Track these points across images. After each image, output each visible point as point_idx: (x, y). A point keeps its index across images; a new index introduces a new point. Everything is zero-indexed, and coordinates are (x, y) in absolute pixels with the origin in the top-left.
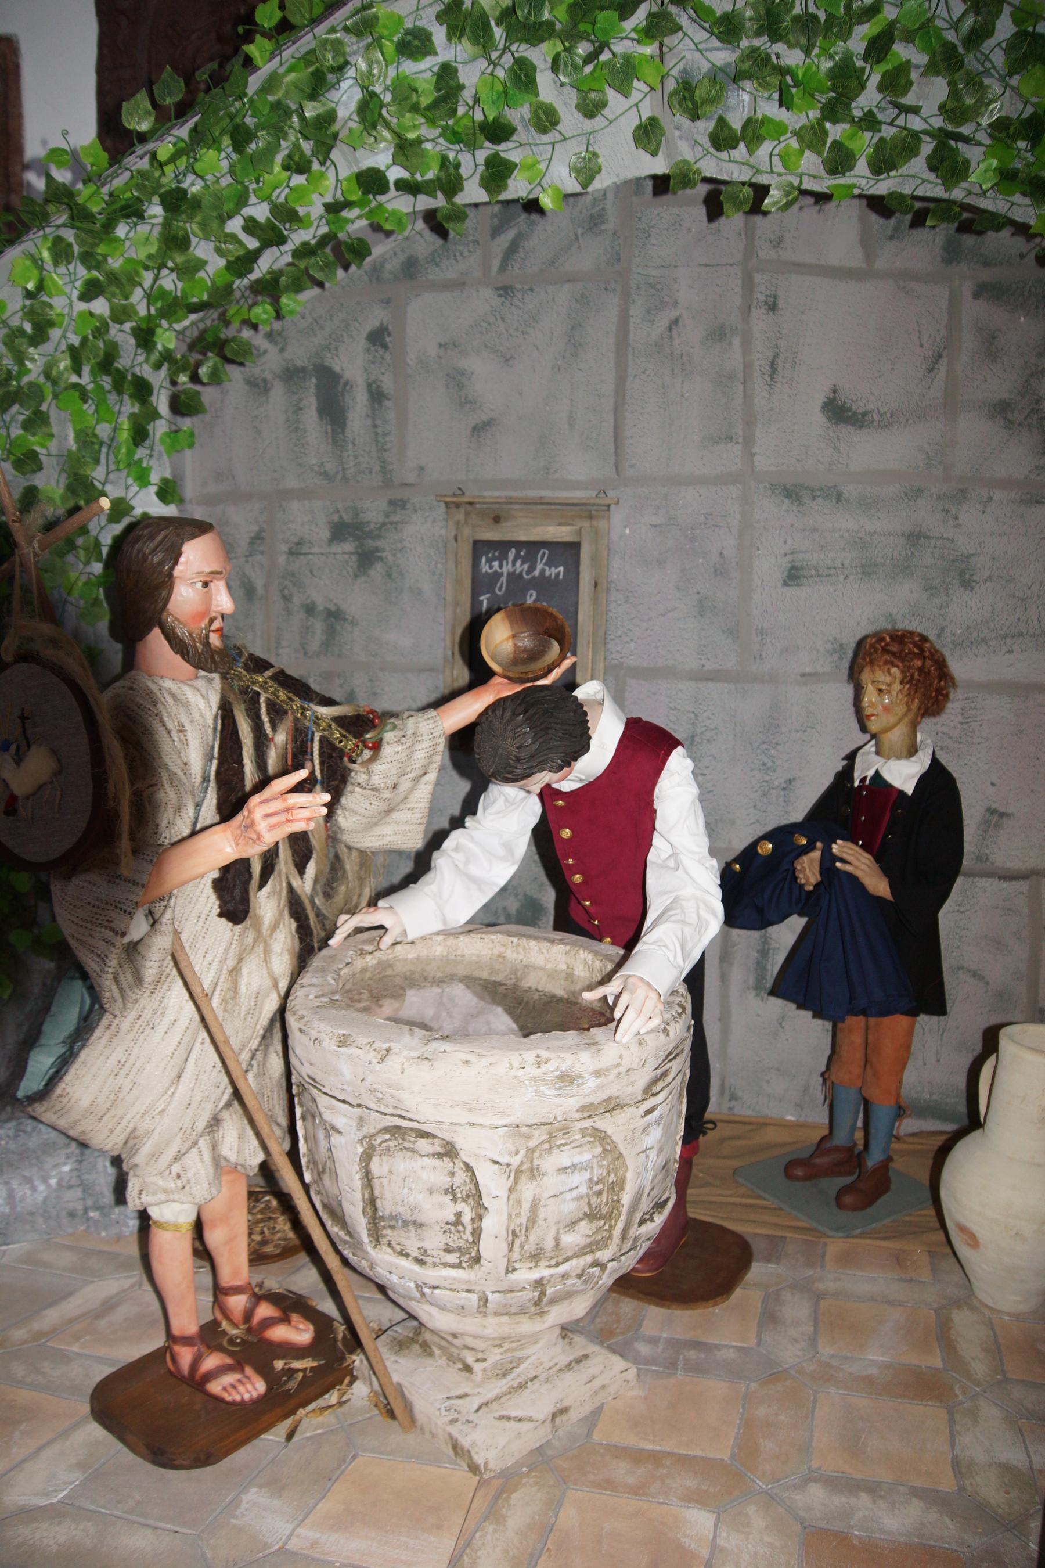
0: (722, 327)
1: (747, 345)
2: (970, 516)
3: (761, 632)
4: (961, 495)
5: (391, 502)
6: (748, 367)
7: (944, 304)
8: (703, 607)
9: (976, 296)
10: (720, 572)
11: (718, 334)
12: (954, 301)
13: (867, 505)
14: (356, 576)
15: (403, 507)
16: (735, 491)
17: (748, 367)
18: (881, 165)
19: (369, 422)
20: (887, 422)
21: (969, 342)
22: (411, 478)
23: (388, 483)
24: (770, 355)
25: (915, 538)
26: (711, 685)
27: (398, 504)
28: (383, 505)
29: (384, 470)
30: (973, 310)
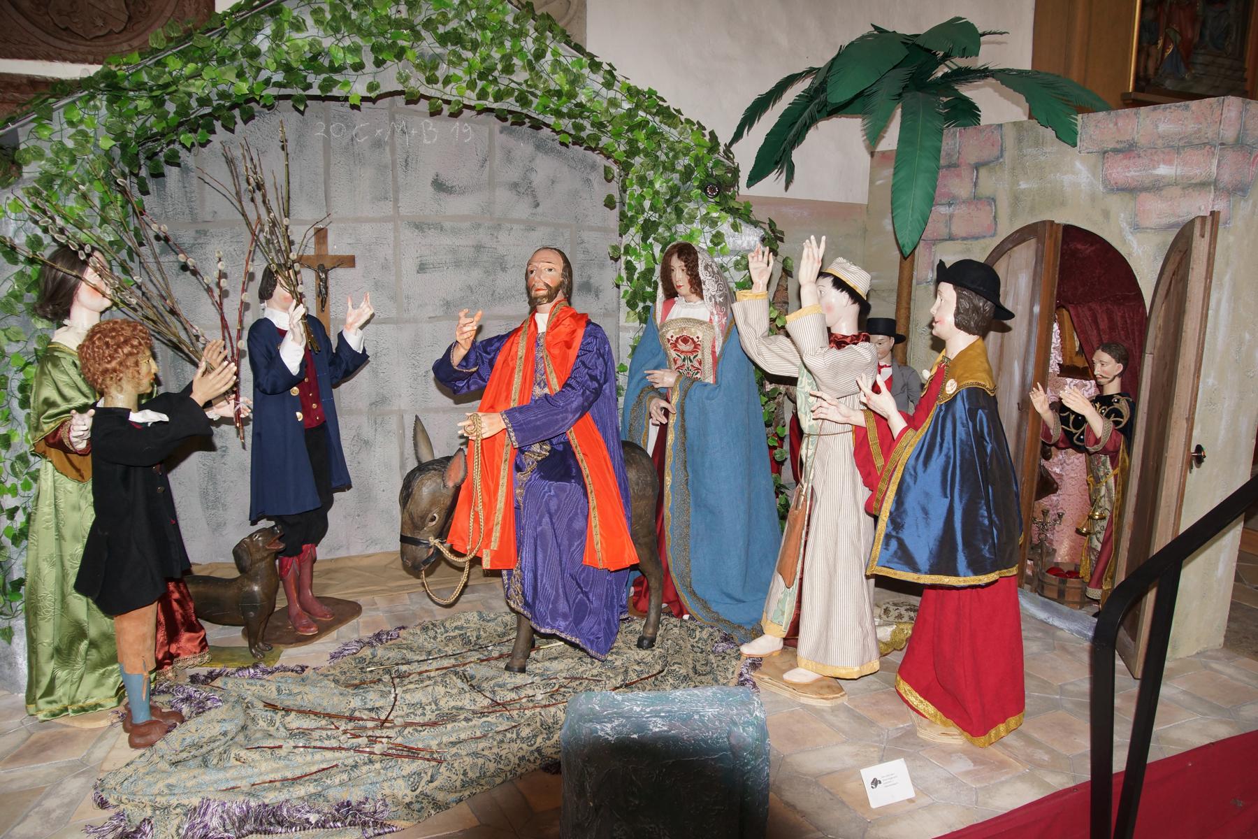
0: (380, 140)
1: (393, 151)
2: (503, 237)
3: (408, 297)
4: (498, 227)
5: (197, 232)
6: (394, 163)
7: (487, 135)
8: (377, 286)
9: (501, 132)
10: (385, 267)
11: (378, 144)
12: (491, 134)
13: (455, 232)
14: (178, 275)
15: (205, 235)
16: (390, 226)
17: (394, 163)
18: (499, 97)
19: (181, 184)
20: (463, 191)
21: (498, 155)
22: (209, 218)
23: (194, 221)
24: (405, 156)
25: (479, 248)
26: (383, 326)
27: (202, 233)
28: (193, 234)
29: (191, 213)
30: (501, 139)
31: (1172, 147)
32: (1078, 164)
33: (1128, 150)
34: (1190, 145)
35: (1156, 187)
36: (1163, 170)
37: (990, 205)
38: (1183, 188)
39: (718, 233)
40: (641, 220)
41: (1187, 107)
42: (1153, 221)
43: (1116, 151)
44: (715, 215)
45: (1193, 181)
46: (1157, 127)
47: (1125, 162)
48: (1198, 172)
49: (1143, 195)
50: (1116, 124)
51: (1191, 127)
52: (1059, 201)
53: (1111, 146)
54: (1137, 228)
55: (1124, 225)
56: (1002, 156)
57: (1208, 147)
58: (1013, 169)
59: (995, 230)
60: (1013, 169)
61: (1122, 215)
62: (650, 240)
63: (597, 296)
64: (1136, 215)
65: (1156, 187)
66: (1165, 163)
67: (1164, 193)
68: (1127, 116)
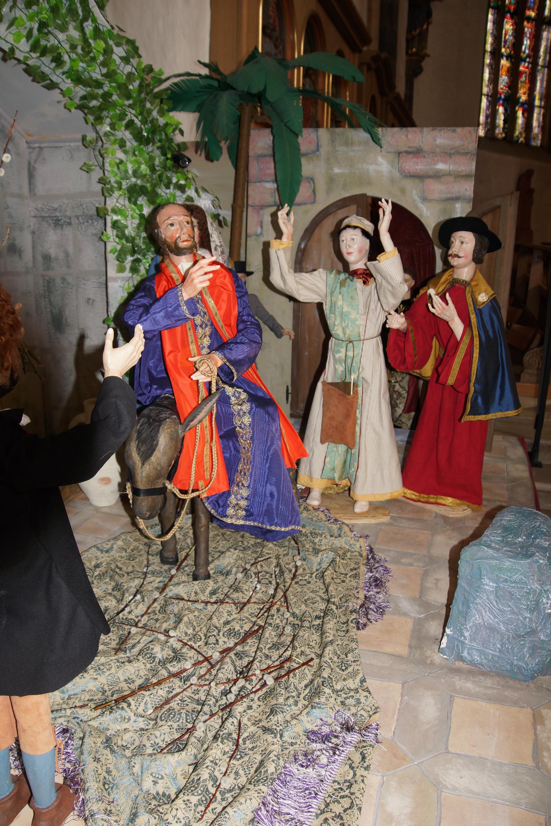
31: (447, 153)
32: (380, 159)
33: (417, 153)
34: (458, 153)
35: (437, 176)
36: (441, 166)
37: (309, 182)
38: (455, 178)
39: (188, 196)
40: (125, 184)
41: (454, 131)
42: (436, 196)
43: (408, 153)
44: (182, 182)
45: (461, 174)
46: (435, 140)
47: (415, 160)
48: (464, 169)
49: (428, 181)
50: (407, 136)
51: (458, 143)
52: (368, 182)
53: (405, 149)
54: (424, 199)
55: (416, 197)
56: (318, 150)
57: (469, 155)
58: (328, 159)
59: (315, 199)
60: (328, 159)
61: (414, 192)
62: (139, 202)
63: (20, 256)
64: (424, 192)
65: (437, 176)
66: (442, 162)
67: (442, 179)
68: (415, 132)
